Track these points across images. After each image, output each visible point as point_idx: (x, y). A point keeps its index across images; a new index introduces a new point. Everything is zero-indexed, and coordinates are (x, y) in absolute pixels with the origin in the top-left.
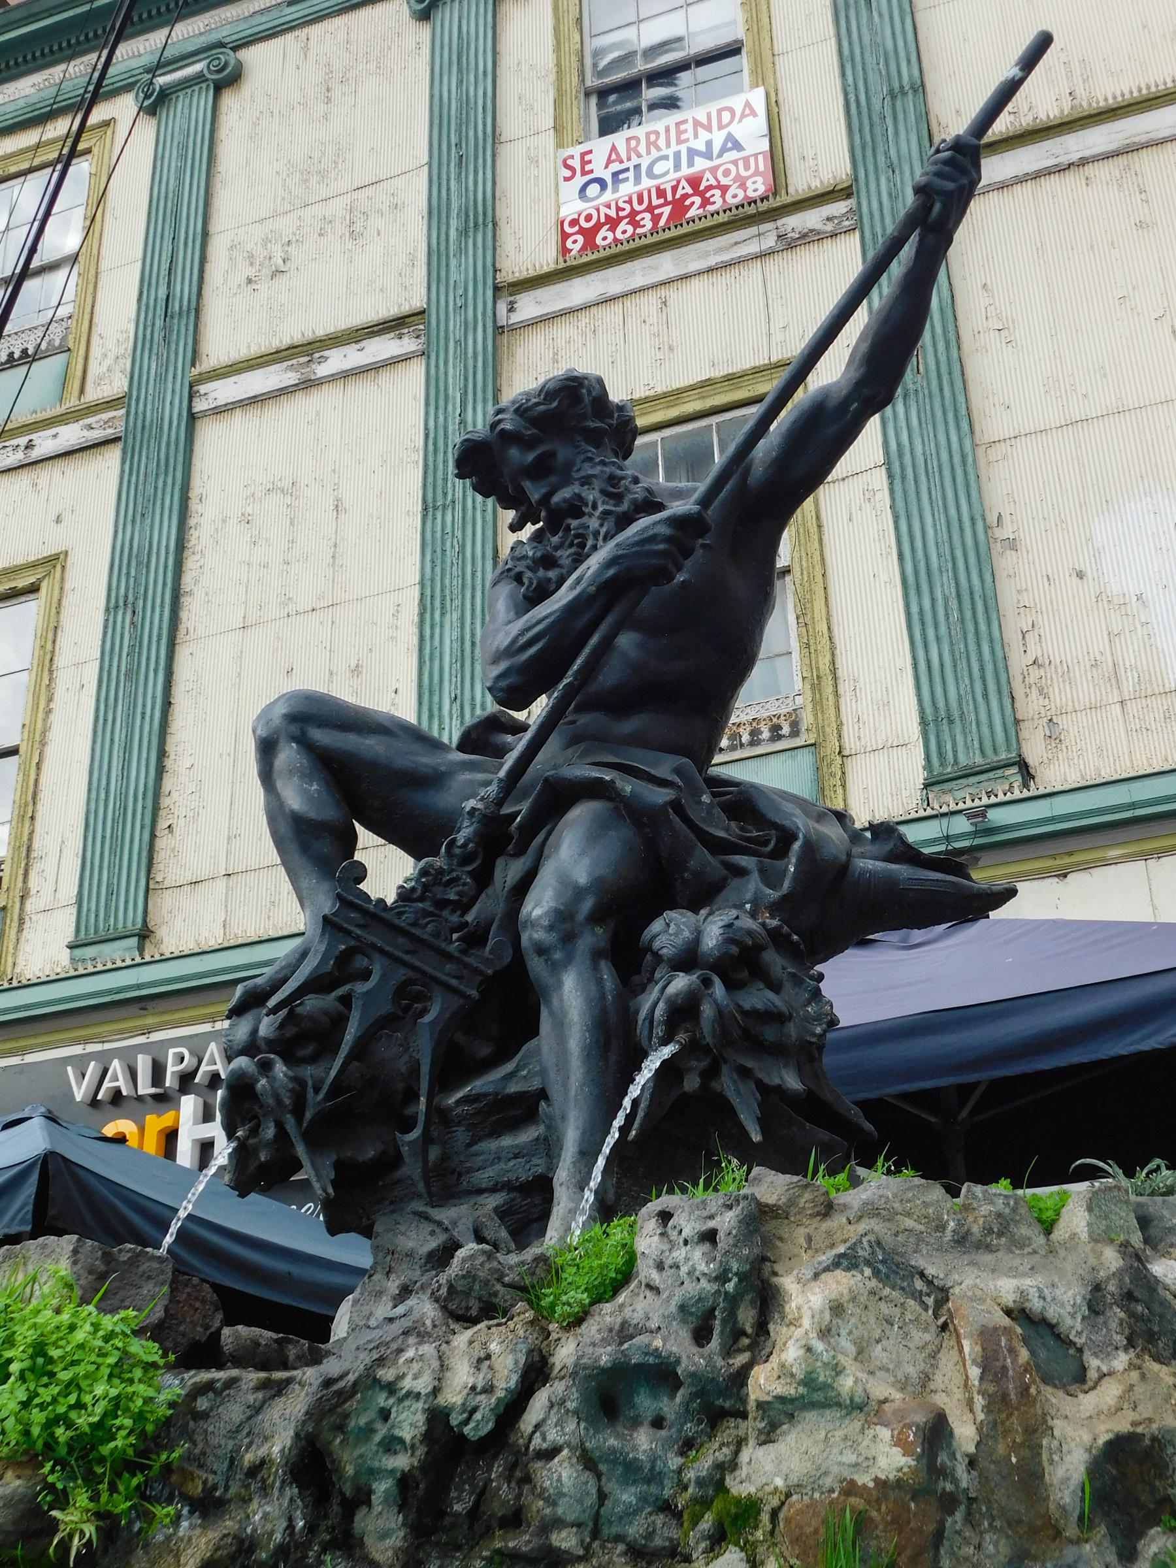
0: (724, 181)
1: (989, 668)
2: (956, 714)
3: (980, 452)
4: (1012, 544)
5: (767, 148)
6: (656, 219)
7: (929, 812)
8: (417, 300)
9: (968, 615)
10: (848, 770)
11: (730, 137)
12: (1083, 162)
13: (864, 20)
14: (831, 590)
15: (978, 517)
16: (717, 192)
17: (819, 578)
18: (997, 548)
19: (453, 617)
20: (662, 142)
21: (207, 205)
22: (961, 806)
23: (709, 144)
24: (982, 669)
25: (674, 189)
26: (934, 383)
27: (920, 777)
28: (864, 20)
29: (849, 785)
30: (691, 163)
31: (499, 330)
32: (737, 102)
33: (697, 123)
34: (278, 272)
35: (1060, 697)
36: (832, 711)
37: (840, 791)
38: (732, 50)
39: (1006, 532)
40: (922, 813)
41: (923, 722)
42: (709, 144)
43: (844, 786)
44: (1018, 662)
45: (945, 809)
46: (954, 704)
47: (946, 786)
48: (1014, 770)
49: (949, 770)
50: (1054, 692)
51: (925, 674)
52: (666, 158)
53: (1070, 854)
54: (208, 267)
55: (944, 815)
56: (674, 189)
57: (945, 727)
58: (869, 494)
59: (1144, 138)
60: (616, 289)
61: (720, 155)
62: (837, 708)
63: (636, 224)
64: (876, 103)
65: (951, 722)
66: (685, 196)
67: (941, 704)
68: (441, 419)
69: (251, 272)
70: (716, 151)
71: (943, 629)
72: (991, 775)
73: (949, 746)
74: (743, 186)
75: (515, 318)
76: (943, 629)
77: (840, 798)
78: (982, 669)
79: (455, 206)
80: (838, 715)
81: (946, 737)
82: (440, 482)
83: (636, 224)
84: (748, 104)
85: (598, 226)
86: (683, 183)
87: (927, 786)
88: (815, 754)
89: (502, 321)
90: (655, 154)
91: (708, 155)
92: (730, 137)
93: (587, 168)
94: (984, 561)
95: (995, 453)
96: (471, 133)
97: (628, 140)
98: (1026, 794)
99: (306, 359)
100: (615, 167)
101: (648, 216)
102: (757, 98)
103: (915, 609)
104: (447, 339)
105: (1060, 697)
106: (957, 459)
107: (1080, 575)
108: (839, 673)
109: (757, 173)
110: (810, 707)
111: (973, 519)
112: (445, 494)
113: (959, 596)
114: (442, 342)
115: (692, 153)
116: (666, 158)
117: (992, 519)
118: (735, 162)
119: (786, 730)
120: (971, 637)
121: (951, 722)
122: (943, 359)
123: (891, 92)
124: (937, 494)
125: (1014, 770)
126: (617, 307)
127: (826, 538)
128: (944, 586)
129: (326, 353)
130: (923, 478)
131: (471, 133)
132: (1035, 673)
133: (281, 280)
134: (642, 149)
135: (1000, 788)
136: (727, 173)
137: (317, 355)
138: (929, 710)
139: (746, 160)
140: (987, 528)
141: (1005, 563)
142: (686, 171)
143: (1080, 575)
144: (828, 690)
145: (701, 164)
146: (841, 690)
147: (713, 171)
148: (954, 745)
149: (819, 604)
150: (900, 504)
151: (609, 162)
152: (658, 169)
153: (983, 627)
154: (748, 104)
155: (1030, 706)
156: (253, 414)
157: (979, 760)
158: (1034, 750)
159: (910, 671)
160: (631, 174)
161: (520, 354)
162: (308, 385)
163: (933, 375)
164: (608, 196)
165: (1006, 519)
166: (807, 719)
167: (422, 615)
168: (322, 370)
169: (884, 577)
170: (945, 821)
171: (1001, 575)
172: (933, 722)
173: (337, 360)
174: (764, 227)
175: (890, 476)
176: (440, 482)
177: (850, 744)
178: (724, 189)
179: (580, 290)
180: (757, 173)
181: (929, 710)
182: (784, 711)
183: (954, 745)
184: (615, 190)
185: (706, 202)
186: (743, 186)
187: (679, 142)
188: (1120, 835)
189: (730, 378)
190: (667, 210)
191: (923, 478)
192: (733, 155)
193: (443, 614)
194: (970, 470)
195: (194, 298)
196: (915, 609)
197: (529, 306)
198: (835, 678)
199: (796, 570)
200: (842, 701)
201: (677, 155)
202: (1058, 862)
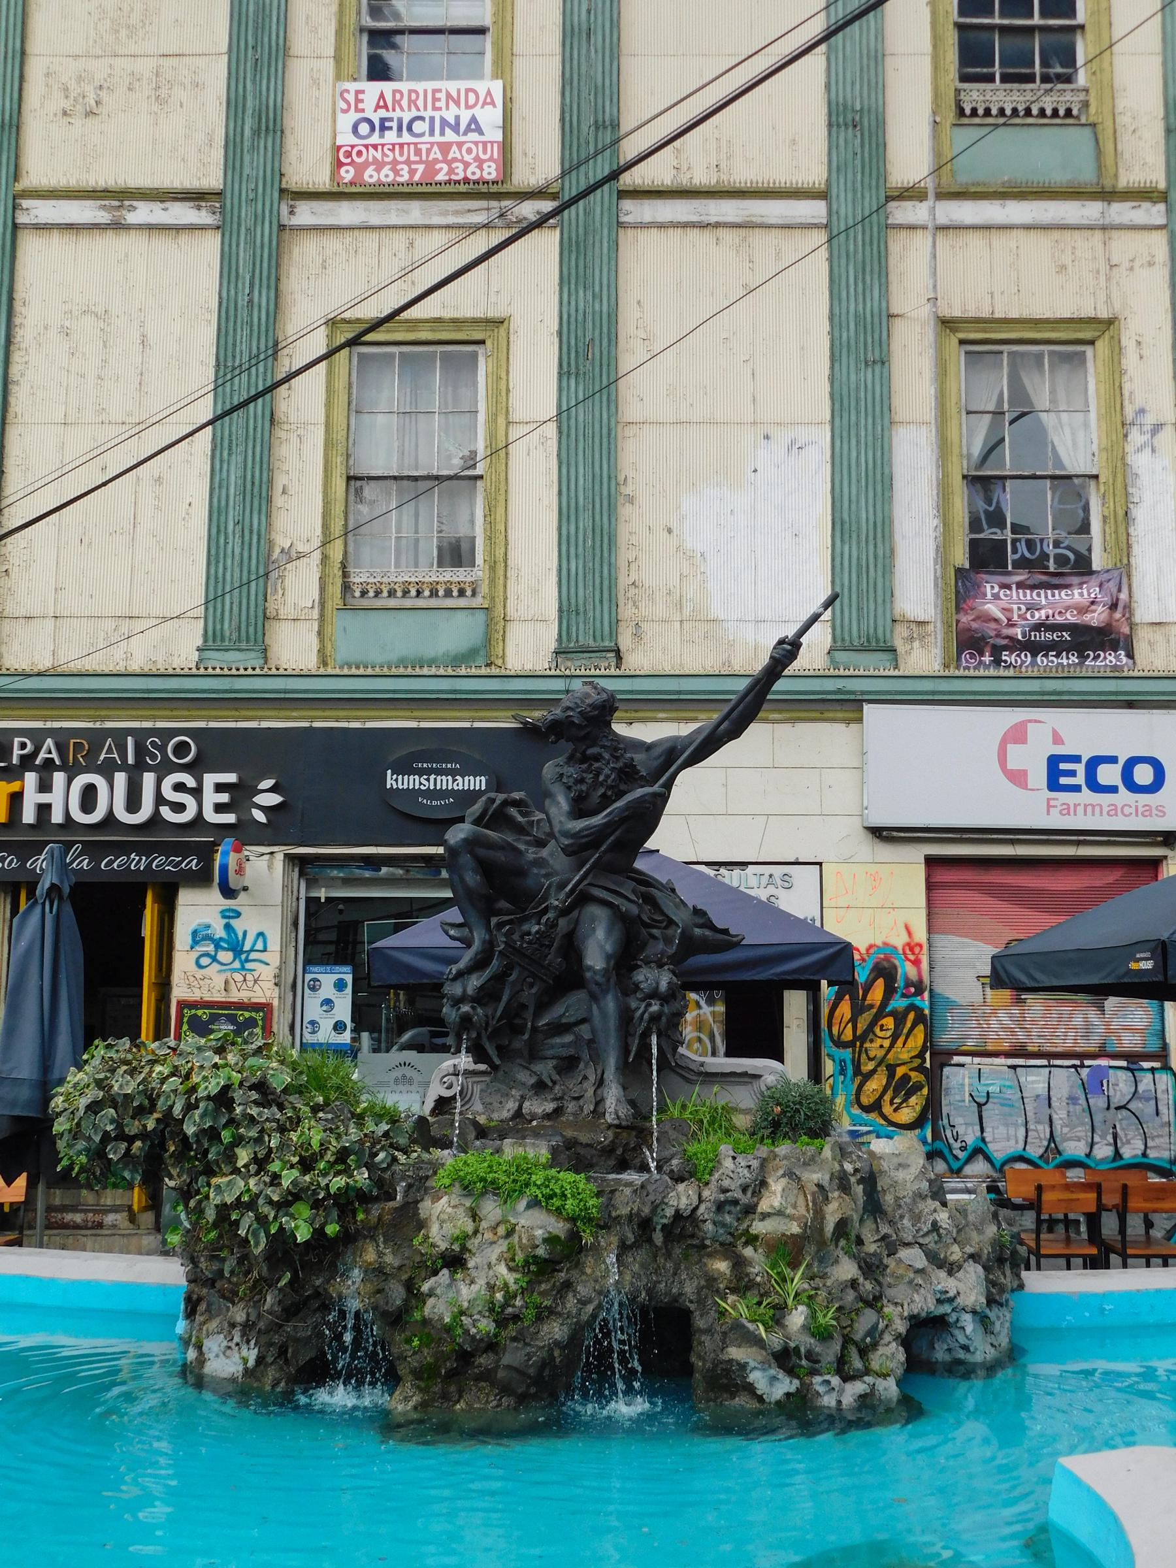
0: (468, 158)
1: (606, 583)
2: (581, 609)
3: (620, 427)
4: (631, 500)
5: (501, 139)
6: (412, 172)
7: (558, 672)
8: (213, 180)
9: (598, 544)
10: (508, 629)
11: (474, 120)
12: (717, 225)
13: (584, 51)
14: (510, 502)
15: (613, 476)
16: (461, 166)
17: (502, 492)
18: (621, 499)
19: (237, 459)
20: (420, 103)
21: (24, 23)
22: (578, 672)
23: (457, 118)
24: (602, 583)
25: (429, 151)
26: (597, 369)
27: (553, 646)
28: (584, 51)
29: (507, 640)
30: (442, 133)
31: (282, 227)
32: (481, 87)
33: (449, 96)
34: (90, 113)
35: (645, 609)
36: (501, 588)
37: (501, 643)
38: (481, 31)
39: (628, 490)
40: (553, 672)
41: (560, 610)
42: (457, 118)
43: (504, 640)
44: (623, 581)
45: (568, 673)
46: (581, 602)
47: (569, 656)
48: (612, 655)
49: (572, 645)
50: (642, 605)
51: (565, 578)
52: (422, 118)
53: (636, 711)
54: (25, 85)
55: (567, 676)
56: (429, 151)
57: (573, 616)
58: (544, 440)
59: (758, 220)
60: (375, 221)
61: (465, 133)
62: (505, 586)
63: (397, 173)
64: (584, 128)
65: (578, 614)
66: (436, 161)
67: (573, 601)
68: (232, 292)
69: (67, 104)
70: (463, 127)
71: (580, 549)
72: (598, 654)
73: (574, 629)
74: (480, 168)
75: (296, 221)
76: (580, 549)
77: (501, 648)
78: (602, 583)
79: (249, 104)
80: (505, 592)
81: (573, 622)
82: (230, 346)
83: (397, 173)
84: (489, 93)
85: (366, 164)
86: (436, 148)
87: (557, 653)
88: (487, 615)
89: (285, 221)
90: (414, 113)
91: (456, 128)
92: (474, 120)
93: (360, 106)
94: (612, 510)
95: (630, 431)
96: (266, 40)
97: (394, 92)
98: (618, 672)
99: (117, 203)
100: (382, 113)
101: (406, 168)
102: (497, 87)
103: (564, 532)
104: (239, 225)
105: (645, 609)
106: (605, 431)
107: (670, 531)
108: (509, 562)
109: (491, 159)
110: (487, 582)
111: (609, 477)
112: (234, 357)
113: (593, 530)
114: (235, 226)
115: (444, 123)
116: (422, 118)
117: (621, 478)
118: (476, 143)
119: (469, 593)
120: (597, 558)
121: (578, 614)
122: (605, 353)
123: (596, 122)
124: (589, 453)
125: (612, 655)
126: (375, 236)
127: (510, 463)
128: (585, 522)
129: (135, 203)
130: (581, 438)
131: (266, 40)
132: (632, 591)
133: (91, 121)
134: (405, 103)
135: (604, 664)
136: (469, 151)
137: (127, 203)
138: (565, 603)
139: (485, 144)
140: (617, 484)
141: (625, 511)
142: (437, 138)
143: (670, 531)
144: (501, 573)
145: (450, 136)
146: (509, 575)
147: (460, 145)
148: (577, 630)
149: (500, 511)
150: (564, 455)
151: (378, 107)
152: (418, 127)
153: (606, 554)
154: (489, 93)
155: (627, 612)
156: (68, 239)
157: (591, 643)
158: (625, 641)
159: (555, 572)
160: (394, 125)
161: (296, 251)
162: (118, 226)
163: (597, 363)
164: (375, 139)
165: (630, 481)
166: (484, 589)
167: (213, 450)
168: (132, 218)
169: (546, 502)
170: (568, 680)
171: (621, 519)
172: (566, 611)
173: (143, 213)
174: (494, 203)
175: (560, 429)
176: (230, 346)
177: (511, 612)
178: (467, 165)
179: (348, 213)
180: (491, 159)
181: (565, 603)
182: (469, 579)
183: (577, 630)
184: (382, 136)
185: (451, 171)
186: (480, 168)
187: (435, 108)
188: (668, 706)
189: (454, 321)
190: (421, 168)
191: (581, 438)
192: (474, 136)
193: (229, 455)
194: (612, 441)
195: (15, 116)
196: (564, 532)
197: (306, 213)
198: (506, 566)
199: (487, 478)
200: (509, 582)
201: (432, 119)
202: (628, 715)
